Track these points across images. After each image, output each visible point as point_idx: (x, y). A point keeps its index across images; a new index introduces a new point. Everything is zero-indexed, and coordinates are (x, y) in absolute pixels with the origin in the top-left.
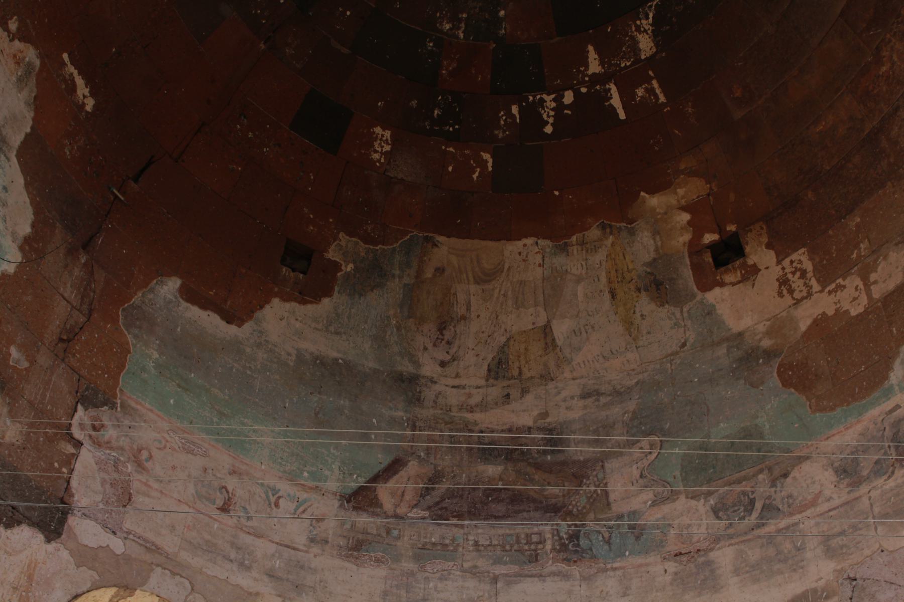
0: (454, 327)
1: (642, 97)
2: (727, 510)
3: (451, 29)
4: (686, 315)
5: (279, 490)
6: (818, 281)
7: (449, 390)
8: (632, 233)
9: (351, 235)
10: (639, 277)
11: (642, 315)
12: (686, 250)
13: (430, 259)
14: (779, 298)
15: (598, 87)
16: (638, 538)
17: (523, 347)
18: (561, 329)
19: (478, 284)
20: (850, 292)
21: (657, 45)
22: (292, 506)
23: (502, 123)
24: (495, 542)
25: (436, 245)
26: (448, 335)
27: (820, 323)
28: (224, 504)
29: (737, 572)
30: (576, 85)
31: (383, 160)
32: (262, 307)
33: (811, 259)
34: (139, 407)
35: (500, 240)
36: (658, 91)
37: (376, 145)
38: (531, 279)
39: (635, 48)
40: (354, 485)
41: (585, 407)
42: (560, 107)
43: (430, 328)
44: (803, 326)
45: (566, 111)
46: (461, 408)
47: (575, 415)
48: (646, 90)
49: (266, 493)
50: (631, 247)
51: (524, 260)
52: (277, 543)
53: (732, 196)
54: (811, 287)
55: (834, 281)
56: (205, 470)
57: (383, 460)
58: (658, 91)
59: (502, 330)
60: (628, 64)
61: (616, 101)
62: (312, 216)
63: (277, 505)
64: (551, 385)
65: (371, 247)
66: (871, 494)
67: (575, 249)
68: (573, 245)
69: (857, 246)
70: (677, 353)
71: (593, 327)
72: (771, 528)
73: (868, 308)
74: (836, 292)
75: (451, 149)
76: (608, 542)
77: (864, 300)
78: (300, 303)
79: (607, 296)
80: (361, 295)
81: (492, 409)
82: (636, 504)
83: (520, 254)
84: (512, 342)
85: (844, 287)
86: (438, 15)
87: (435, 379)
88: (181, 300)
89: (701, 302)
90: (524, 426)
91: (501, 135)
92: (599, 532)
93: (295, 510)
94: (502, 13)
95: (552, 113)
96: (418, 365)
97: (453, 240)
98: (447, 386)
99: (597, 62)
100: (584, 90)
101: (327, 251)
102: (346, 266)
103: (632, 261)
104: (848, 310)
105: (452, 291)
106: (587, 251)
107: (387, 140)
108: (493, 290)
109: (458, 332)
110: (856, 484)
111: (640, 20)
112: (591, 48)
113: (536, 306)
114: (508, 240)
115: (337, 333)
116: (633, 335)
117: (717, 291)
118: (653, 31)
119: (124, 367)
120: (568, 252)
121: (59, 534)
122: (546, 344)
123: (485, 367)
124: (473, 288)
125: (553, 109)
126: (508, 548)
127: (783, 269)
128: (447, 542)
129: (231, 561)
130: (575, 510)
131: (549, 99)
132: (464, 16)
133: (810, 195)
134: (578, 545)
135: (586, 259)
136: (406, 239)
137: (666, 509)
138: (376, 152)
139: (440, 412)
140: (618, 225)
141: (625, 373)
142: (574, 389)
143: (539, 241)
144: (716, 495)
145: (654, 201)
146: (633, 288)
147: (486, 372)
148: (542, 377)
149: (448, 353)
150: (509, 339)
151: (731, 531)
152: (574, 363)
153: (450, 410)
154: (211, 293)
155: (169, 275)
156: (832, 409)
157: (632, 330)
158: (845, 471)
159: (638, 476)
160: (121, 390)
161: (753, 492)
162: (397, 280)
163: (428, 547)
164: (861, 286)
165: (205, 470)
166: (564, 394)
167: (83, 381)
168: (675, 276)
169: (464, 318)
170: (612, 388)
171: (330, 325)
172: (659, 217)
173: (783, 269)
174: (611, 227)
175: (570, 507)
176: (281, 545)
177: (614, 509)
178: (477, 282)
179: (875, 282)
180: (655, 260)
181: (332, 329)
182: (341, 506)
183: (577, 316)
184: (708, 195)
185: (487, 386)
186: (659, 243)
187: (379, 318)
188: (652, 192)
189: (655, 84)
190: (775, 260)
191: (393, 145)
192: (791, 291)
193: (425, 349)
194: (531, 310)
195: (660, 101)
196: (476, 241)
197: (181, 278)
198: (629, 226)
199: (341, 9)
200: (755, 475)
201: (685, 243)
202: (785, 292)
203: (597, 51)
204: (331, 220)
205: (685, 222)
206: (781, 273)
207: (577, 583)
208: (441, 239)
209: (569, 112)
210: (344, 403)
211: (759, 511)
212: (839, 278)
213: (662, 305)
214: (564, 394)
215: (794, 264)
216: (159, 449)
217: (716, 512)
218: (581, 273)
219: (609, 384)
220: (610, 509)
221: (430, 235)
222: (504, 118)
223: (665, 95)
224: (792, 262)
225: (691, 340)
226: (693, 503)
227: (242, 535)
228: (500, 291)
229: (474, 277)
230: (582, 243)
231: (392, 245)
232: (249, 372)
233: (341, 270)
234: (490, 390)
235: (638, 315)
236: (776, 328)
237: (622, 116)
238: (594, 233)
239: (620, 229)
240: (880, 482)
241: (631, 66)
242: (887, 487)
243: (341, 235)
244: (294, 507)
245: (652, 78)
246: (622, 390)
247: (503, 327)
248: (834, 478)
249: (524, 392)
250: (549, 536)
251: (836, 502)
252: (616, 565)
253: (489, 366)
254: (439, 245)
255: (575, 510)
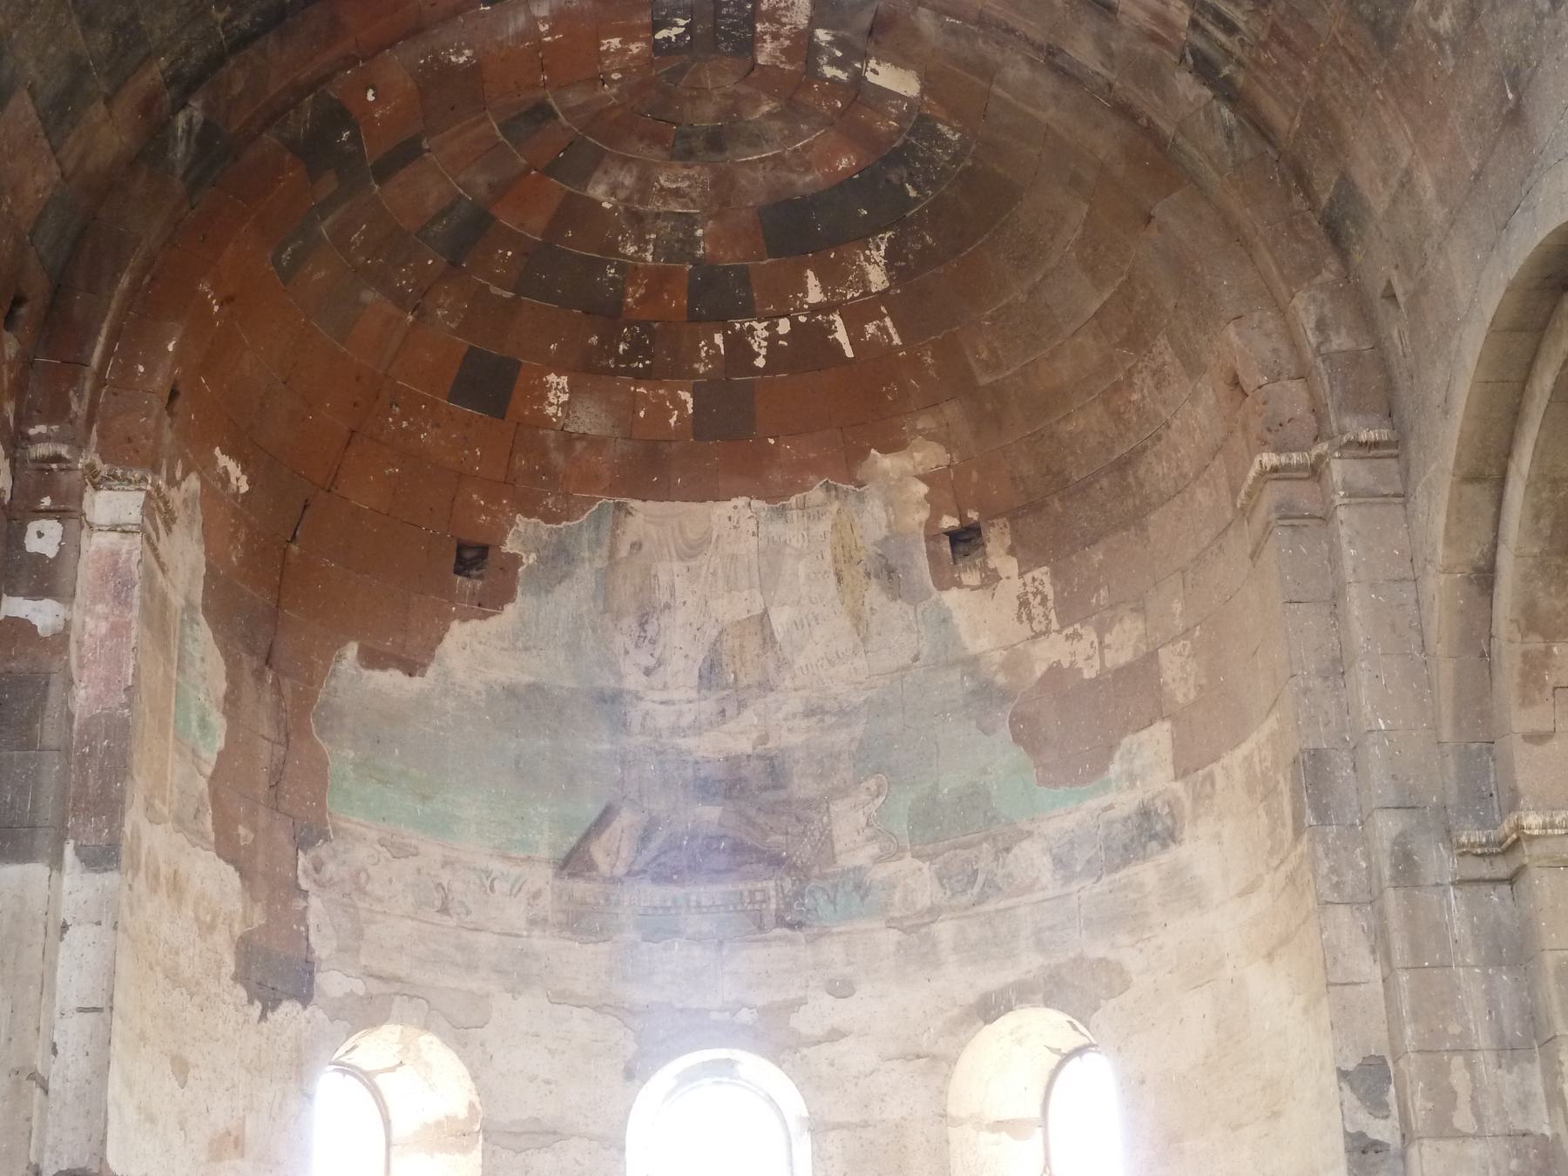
0: (657, 619)
1: (872, 334)
2: (951, 877)
3: (636, 252)
4: (919, 617)
5: (492, 871)
6: (1057, 615)
7: (656, 706)
8: (861, 498)
9: (528, 514)
10: (869, 558)
11: (871, 609)
12: (922, 532)
13: (623, 533)
14: (1018, 624)
15: (820, 317)
16: (862, 899)
17: (737, 642)
18: (780, 620)
19: (682, 560)
20: (1082, 647)
21: (890, 279)
22: (507, 887)
23: (703, 354)
24: (718, 903)
25: (630, 513)
26: (651, 629)
27: (1055, 673)
28: (443, 903)
29: (955, 949)
30: (795, 311)
31: (560, 414)
32: (440, 639)
33: (1053, 584)
34: (348, 825)
35: (703, 501)
36: (892, 331)
37: (551, 396)
38: (744, 552)
39: (863, 280)
40: (566, 848)
41: (809, 729)
42: (773, 339)
43: (629, 622)
44: (1040, 670)
45: (781, 342)
46: (675, 730)
47: (796, 739)
48: (878, 327)
49: (480, 878)
50: (860, 518)
51: (735, 527)
52: (499, 933)
53: (975, 475)
54: (1050, 622)
55: (1072, 624)
56: (419, 871)
57: (591, 810)
58: (892, 331)
59: (713, 620)
60: (856, 295)
61: (841, 335)
62: (482, 503)
63: (492, 889)
64: (771, 697)
65: (554, 526)
66: (1081, 893)
67: (794, 514)
68: (792, 509)
69: (1097, 590)
70: (906, 668)
71: (816, 619)
72: (989, 907)
73: (1100, 675)
74: (1073, 639)
75: (642, 390)
76: (833, 902)
77: (1097, 666)
78: (480, 618)
79: (833, 578)
80: (547, 592)
81: (706, 730)
82: (862, 857)
83: (730, 518)
84: (725, 637)
85: (1081, 636)
86: (620, 238)
87: (640, 694)
88: (362, 670)
89: (937, 602)
90: (742, 754)
91: (702, 370)
92: (823, 889)
93: (511, 890)
94: (699, 232)
95: (765, 344)
96: (620, 676)
97: (650, 504)
98: (653, 702)
99: (818, 289)
100: (802, 319)
101: (503, 543)
102: (527, 558)
103: (861, 537)
104: (1081, 669)
105: (652, 573)
106: (809, 517)
107: (563, 388)
108: (700, 567)
109: (662, 626)
110: (1067, 880)
111: (870, 250)
112: (810, 273)
113: (751, 588)
114: (716, 500)
115: (526, 649)
116: (862, 636)
117: (954, 592)
118: (885, 264)
119: (326, 784)
120: (786, 517)
121: (311, 996)
122: (764, 639)
123: (696, 673)
124: (677, 566)
125: (765, 339)
126: (731, 908)
127: (1025, 585)
128: (669, 904)
129: (457, 965)
130: (799, 862)
131: (760, 328)
132: (653, 236)
133: (1057, 505)
134: (803, 905)
135: (808, 529)
136: (594, 509)
137: (892, 867)
138: (551, 404)
139: (649, 739)
140: (845, 486)
141: (852, 686)
142: (795, 704)
143: (752, 503)
144: (941, 858)
145: (886, 463)
146: (862, 571)
147: (697, 679)
148: (760, 684)
149: (652, 655)
150: (721, 633)
151: (954, 902)
152: (796, 667)
153: (660, 736)
154: (388, 644)
155: (344, 643)
156: (1056, 786)
157: (861, 627)
158: (1061, 861)
159: (864, 825)
160: (330, 813)
161: (977, 863)
162: (587, 564)
163: (650, 912)
164: (1096, 644)
165: (419, 871)
166: (786, 709)
167: (297, 822)
168: (909, 563)
169: (668, 606)
170: (837, 705)
171: (517, 640)
172: (892, 483)
173: (1025, 585)
174: (836, 488)
175: (794, 858)
176: (503, 934)
177: (839, 862)
178: (681, 559)
179: (1109, 647)
180: (887, 538)
181: (520, 644)
182: (556, 876)
183: (799, 602)
184: (949, 466)
185: (699, 700)
186: (893, 517)
187: (570, 619)
188: (885, 450)
189: (888, 322)
190: (1016, 571)
191: (571, 392)
192: (1031, 619)
193: (627, 652)
194: (746, 593)
195: (894, 343)
196: (677, 503)
197: (356, 639)
198: (858, 490)
199: (500, 251)
200: (980, 843)
201: (921, 523)
202: (1024, 616)
203: (817, 275)
204: (505, 502)
205: (923, 496)
206: (1022, 590)
207: (803, 947)
208: (636, 504)
209: (786, 344)
210: (544, 743)
211: (981, 885)
212: (1077, 622)
213: (894, 599)
214: (786, 709)
215: (1036, 584)
216: (375, 864)
217: (941, 878)
218: (802, 547)
219: (835, 699)
220: (835, 862)
221: (623, 500)
222: (705, 348)
223: (901, 336)
224: (1034, 579)
225: (925, 651)
226: (918, 863)
227: (464, 933)
228: (708, 568)
229: (677, 551)
230: (803, 507)
231: (578, 519)
232: (442, 734)
233: (523, 564)
234: (703, 703)
235: (867, 607)
236: (1015, 662)
237: (849, 353)
238: (816, 495)
239: (846, 492)
240: (1088, 883)
241: (857, 298)
242: (1095, 891)
243: (519, 516)
244: (509, 887)
245: (884, 316)
246: (848, 709)
247: (713, 615)
248: (1051, 866)
249: (742, 705)
250: (773, 893)
251: (1049, 893)
252: (842, 929)
253: (700, 670)
254: (634, 513)
255: (799, 862)
